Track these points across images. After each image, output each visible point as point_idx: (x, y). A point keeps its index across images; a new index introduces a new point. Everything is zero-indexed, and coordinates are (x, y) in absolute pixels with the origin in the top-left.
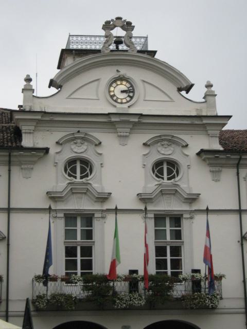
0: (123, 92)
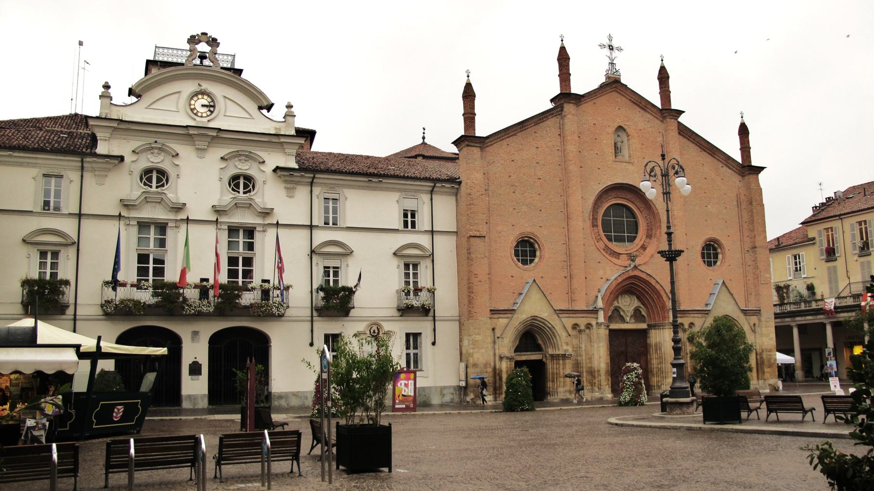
0: (203, 106)
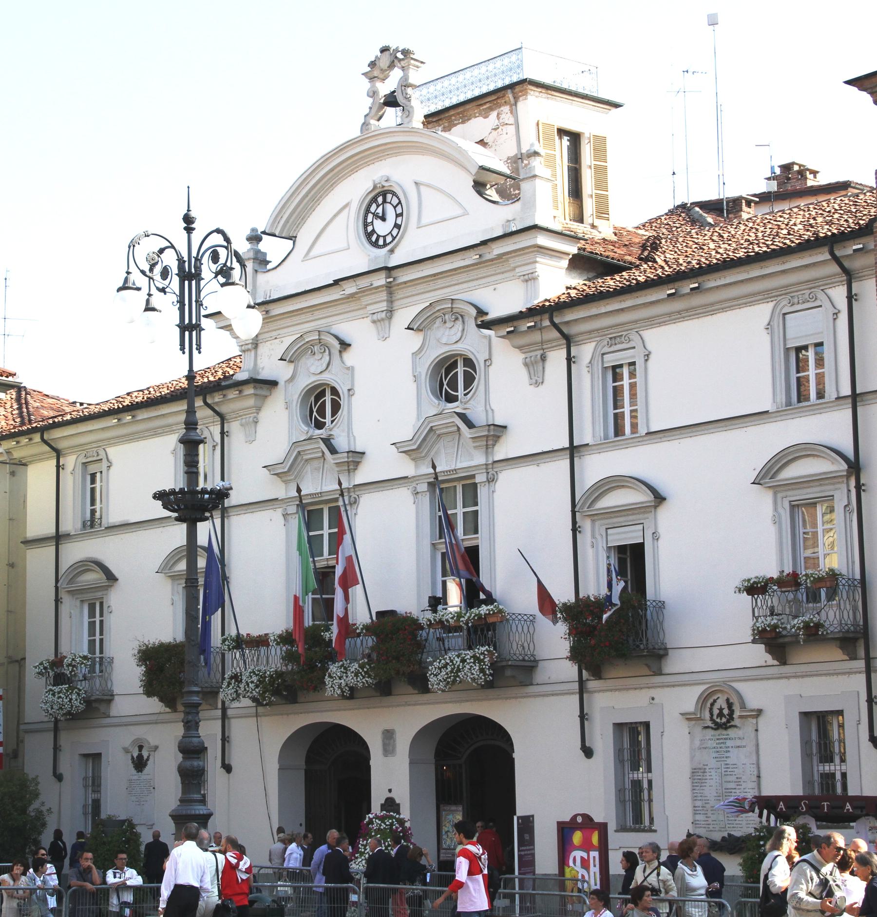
0: (383, 219)
